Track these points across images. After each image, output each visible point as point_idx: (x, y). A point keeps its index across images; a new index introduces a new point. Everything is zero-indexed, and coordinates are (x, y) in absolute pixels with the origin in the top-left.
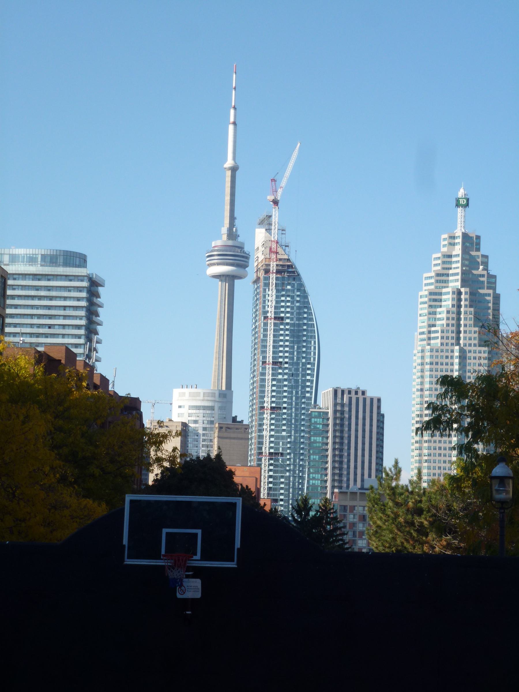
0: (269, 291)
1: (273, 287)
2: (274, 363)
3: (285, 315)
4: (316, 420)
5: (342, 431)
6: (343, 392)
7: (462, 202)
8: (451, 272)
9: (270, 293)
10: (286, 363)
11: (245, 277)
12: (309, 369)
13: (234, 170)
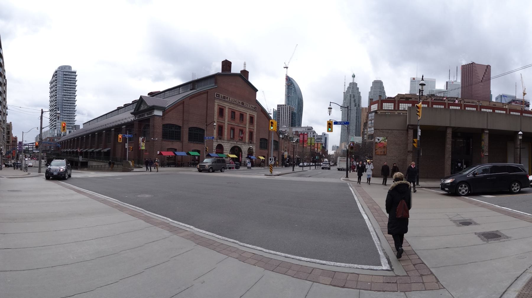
6: (280, 105)
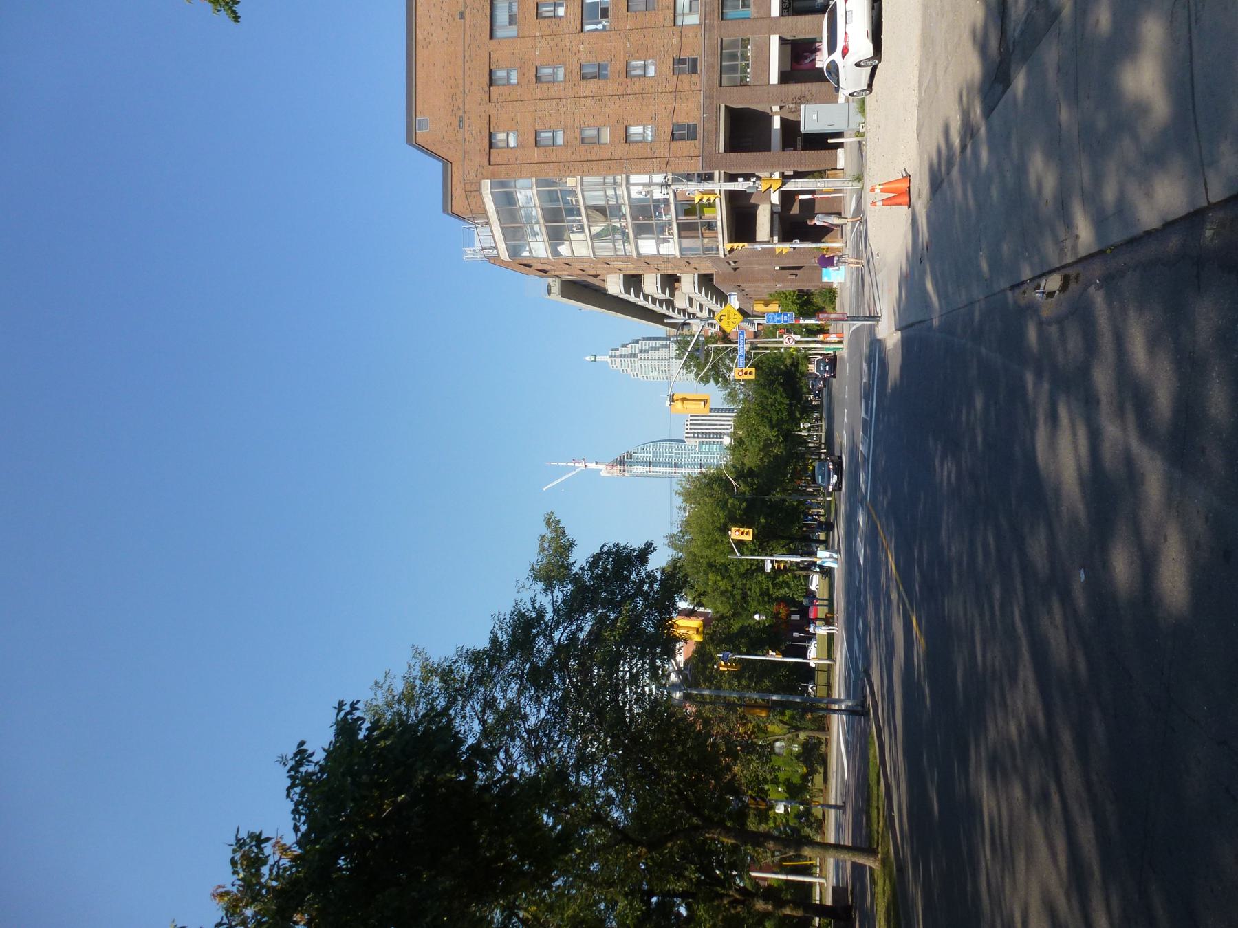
2: (675, 467)
5: (710, 433)
13: (597, 463)
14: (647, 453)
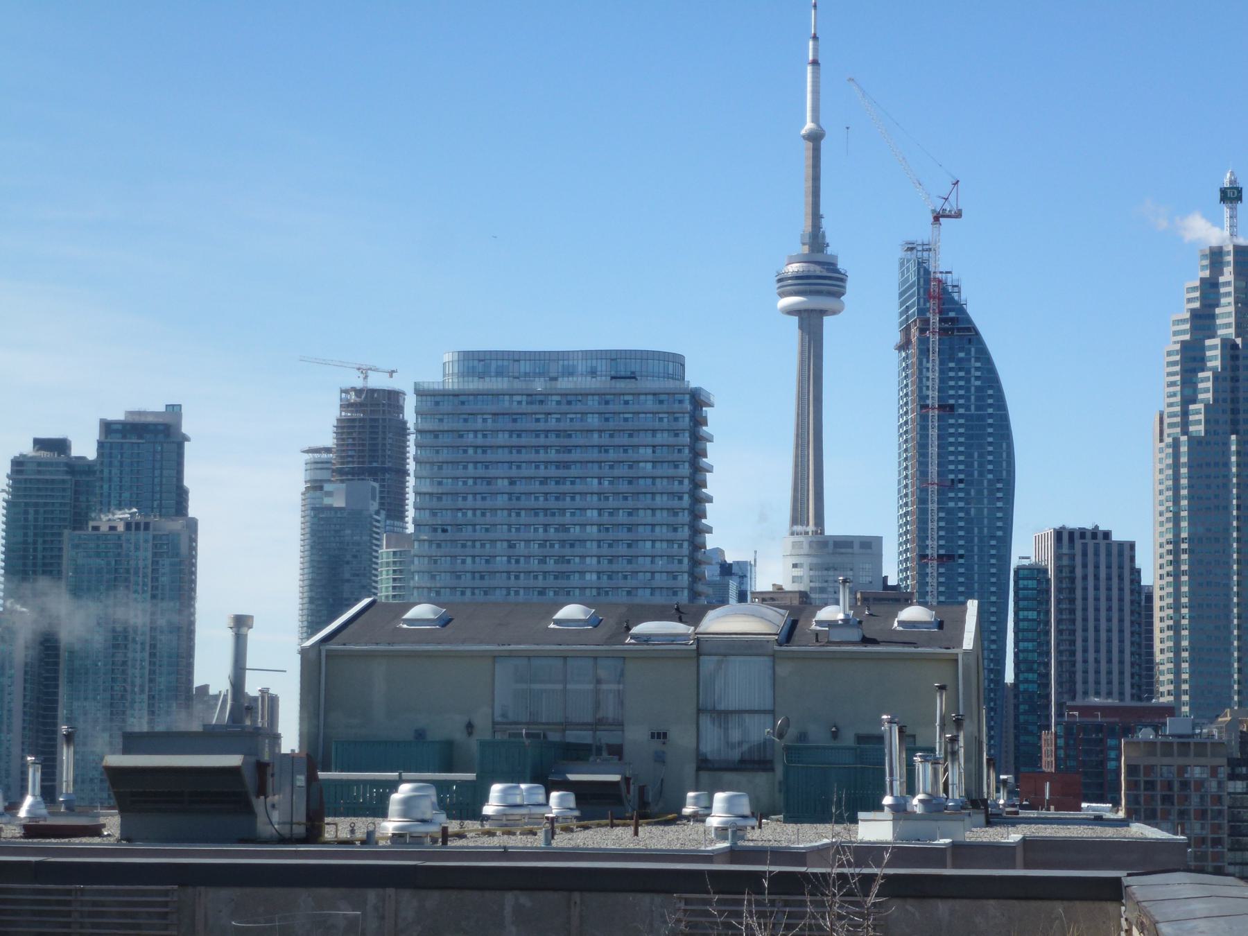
0: (928, 362)
1: (934, 357)
3: (956, 401)
4: (1025, 582)
6: (1072, 533)
7: (1230, 194)
8: (1218, 311)
9: (930, 365)
10: (961, 481)
11: (840, 312)
12: (999, 490)
14: (978, 399)
